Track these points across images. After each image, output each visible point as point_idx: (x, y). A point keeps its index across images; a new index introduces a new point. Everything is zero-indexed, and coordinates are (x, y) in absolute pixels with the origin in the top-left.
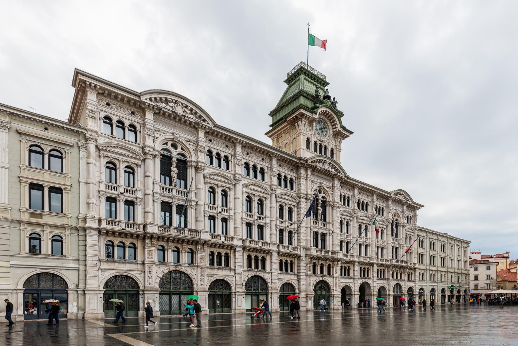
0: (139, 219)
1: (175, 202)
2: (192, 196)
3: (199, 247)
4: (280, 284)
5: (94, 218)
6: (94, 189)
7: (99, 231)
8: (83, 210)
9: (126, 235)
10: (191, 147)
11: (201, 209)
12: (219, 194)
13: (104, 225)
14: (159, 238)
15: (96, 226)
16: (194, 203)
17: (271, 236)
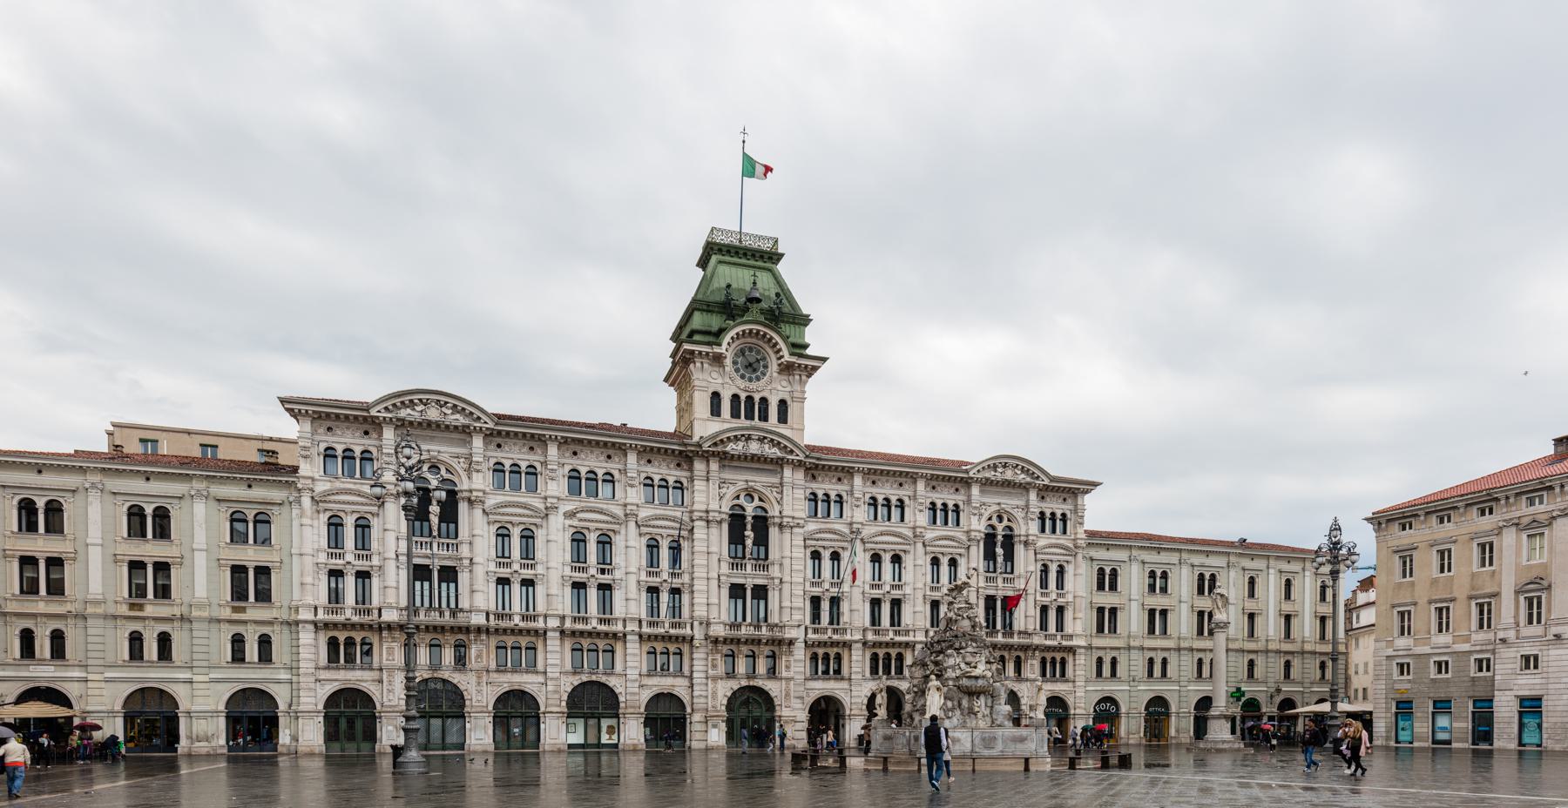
0: (376, 602)
1: (436, 565)
2: (464, 551)
3: (472, 637)
4: (646, 696)
5: (309, 606)
6: (308, 561)
7: (315, 624)
8: (296, 596)
9: (353, 626)
10: (459, 466)
11: (479, 571)
13: (321, 616)
14: (401, 627)
15: (310, 617)
16: (466, 562)
17: (629, 604)
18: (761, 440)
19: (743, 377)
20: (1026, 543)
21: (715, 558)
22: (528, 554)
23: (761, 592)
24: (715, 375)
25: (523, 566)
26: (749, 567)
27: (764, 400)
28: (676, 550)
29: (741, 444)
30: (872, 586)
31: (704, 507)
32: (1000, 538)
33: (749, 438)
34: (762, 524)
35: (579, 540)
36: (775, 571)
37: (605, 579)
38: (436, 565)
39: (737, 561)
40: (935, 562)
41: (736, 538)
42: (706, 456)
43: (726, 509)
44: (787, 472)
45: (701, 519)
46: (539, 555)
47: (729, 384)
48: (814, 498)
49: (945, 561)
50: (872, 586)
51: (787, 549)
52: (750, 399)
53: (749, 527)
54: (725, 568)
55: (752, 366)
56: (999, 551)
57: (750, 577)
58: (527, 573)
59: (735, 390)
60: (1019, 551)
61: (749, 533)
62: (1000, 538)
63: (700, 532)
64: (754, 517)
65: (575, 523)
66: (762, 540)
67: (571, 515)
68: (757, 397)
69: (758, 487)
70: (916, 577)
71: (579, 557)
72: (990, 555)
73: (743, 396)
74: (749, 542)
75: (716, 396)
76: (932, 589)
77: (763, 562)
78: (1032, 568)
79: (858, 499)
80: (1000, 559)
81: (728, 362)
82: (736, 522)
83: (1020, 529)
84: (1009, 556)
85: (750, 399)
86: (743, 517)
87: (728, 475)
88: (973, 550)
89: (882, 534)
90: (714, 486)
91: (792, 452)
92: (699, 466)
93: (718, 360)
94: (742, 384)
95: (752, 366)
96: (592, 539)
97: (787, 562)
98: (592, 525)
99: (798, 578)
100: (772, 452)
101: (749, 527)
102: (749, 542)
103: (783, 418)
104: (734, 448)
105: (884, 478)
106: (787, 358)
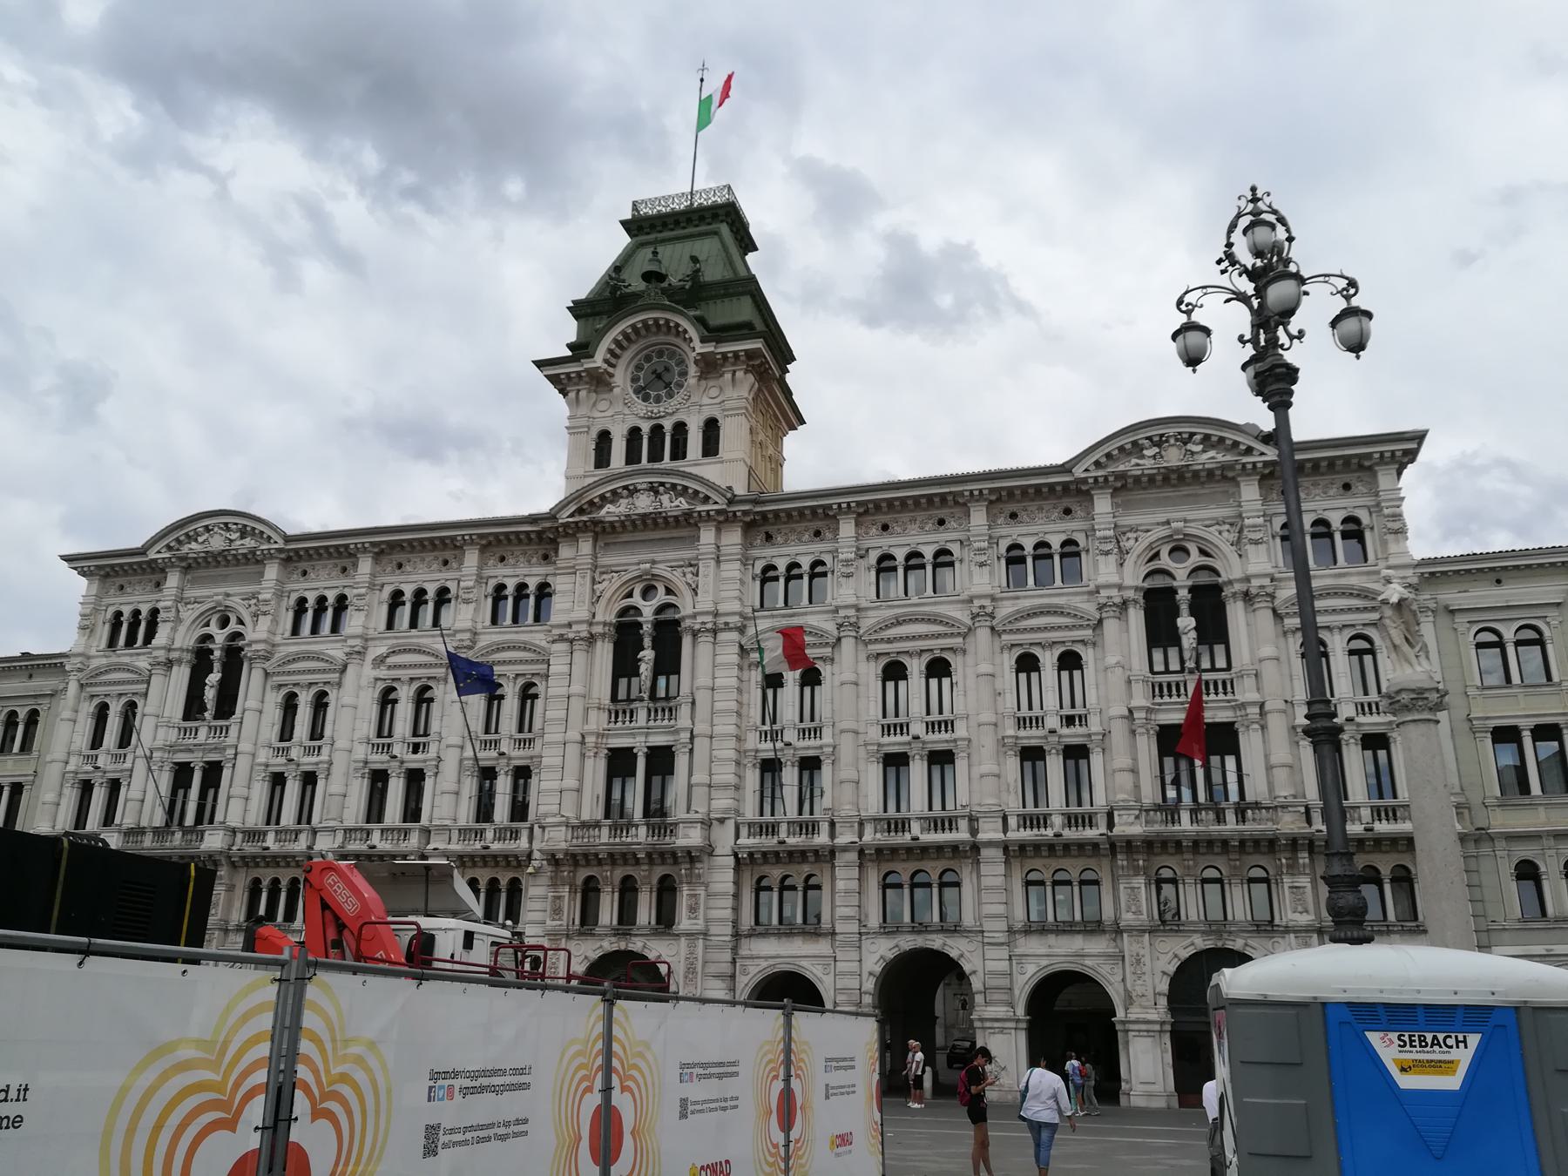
11: (243, 763)
12: (303, 712)
18: (654, 489)
19: (646, 399)
20: (1247, 597)
21: (577, 706)
22: (316, 733)
23: (661, 761)
24: (603, 405)
25: (309, 751)
26: (642, 715)
27: (680, 428)
28: (528, 695)
29: (623, 502)
30: (887, 729)
31: (564, 619)
32: (1183, 595)
33: (632, 491)
34: (669, 634)
35: (387, 699)
36: (683, 719)
37: (415, 761)
38: (197, 760)
39: (620, 706)
40: (1027, 664)
41: (624, 666)
42: (571, 532)
43: (612, 618)
44: (707, 535)
45: (562, 639)
46: (327, 732)
47: (622, 413)
48: (767, 575)
49: (1048, 660)
50: (887, 729)
51: (712, 674)
52: (657, 430)
53: (647, 642)
54: (598, 721)
55: (657, 380)
56: (1186, 622)
57: (640, 736)
58: (308, 763)
59: (633, 421)
60: (1236, 615)
61: (648, 654)
62: (1183, 595)
63: (558, 667)
64: (658, 625)
65: (383, 673)
66: (668, 663)
67: (380, 661)
68: (668, 424)
69: (661, 569)
70: (982, 696)
71: (384, 728)
72: (1161, 633)
73: (646, 427)
74: (645, 669)
75: (604, 438)
76: (1022, 722)
77: (664, 705)
78: (1268, 651)
79: (847, 563)
80: (1189, 640)
81: (621, 377)
82: (626, 635)
83: (1231, 568)
84: (1214, 630)
85: (657, 430)
86: (640, 625)
87: (607, 560)
88: (1111, 626)
89: (899, 622)
90: (583, 584)
91: (707, 499)
92: (565, 551)
93: (599, 382)
94: (641, 407)
95: (657, 380)
96: (405, 694)
97: (702, 698)
98: (404, 674)
99: (726, 726)
100: (672, 505)
101: (647, 642)
102: (645, 669)
103: (711, 446)
104: (610, 512)
105: (905, 517)
106: (701, 348)
